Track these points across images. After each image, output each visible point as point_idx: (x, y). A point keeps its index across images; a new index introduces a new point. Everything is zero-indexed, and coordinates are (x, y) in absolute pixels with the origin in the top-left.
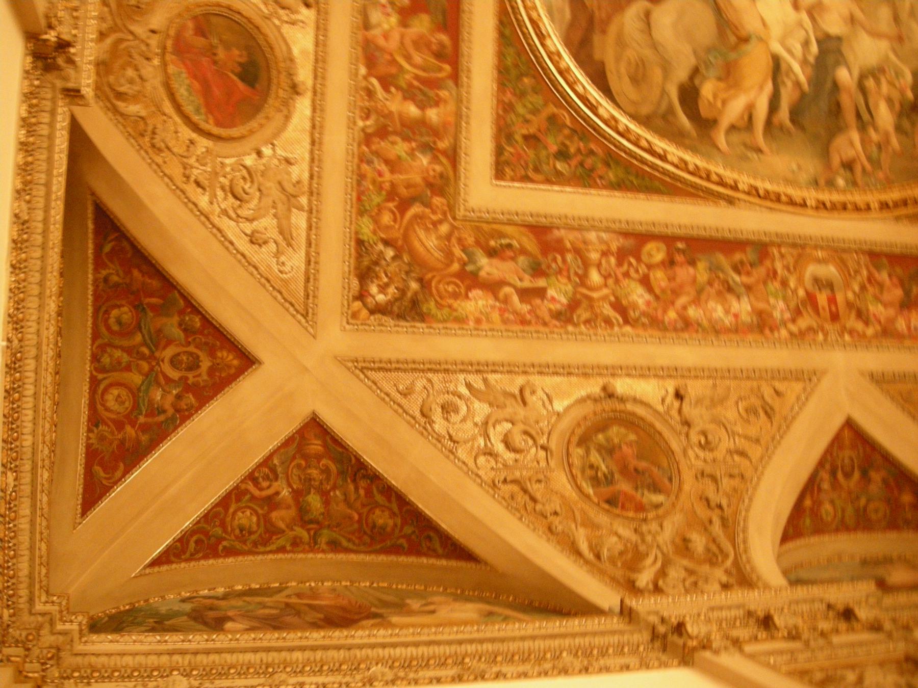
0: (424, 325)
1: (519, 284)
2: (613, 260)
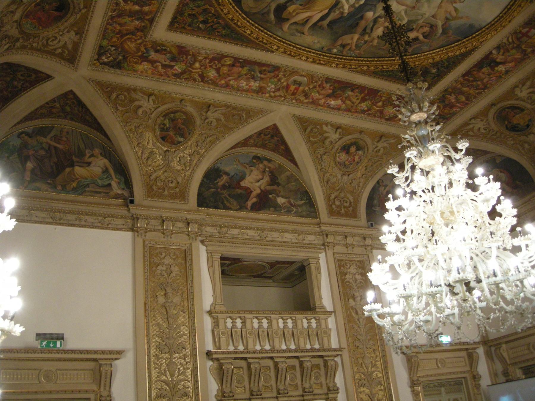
0: (120, 71)
1: (164, 63)
2: (208, 61)
